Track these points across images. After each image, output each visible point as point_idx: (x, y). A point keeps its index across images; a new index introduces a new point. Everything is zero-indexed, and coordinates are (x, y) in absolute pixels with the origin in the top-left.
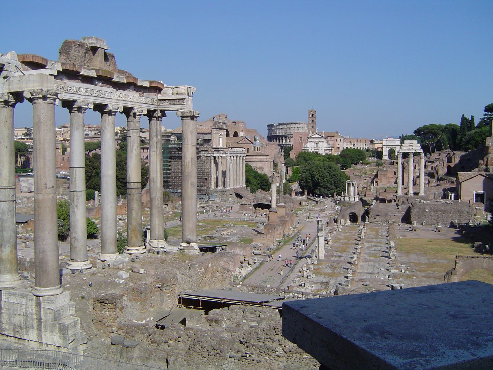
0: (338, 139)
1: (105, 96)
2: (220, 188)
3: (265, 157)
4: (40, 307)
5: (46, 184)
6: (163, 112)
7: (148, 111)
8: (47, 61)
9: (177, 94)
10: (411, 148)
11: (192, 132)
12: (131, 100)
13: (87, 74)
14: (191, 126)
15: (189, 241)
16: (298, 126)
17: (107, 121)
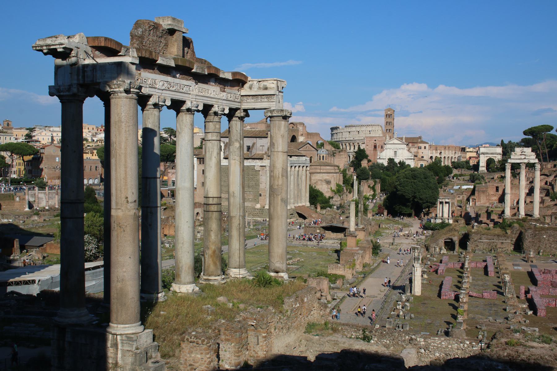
0: (423, 145)
1: (183, 91)
3: (332, 168)
4: (117, 349)
5: (127, 198)
6: (246, 110)
7: (230, 109)
8: (120, 45)
9: (266, 88)
10: (523, 157)
11: (283, 136)
12: (212, 96)
13: (165, 63)
14: (282, 128)
15: (278, 270)
16: (370, 128)
17: (184, 121)
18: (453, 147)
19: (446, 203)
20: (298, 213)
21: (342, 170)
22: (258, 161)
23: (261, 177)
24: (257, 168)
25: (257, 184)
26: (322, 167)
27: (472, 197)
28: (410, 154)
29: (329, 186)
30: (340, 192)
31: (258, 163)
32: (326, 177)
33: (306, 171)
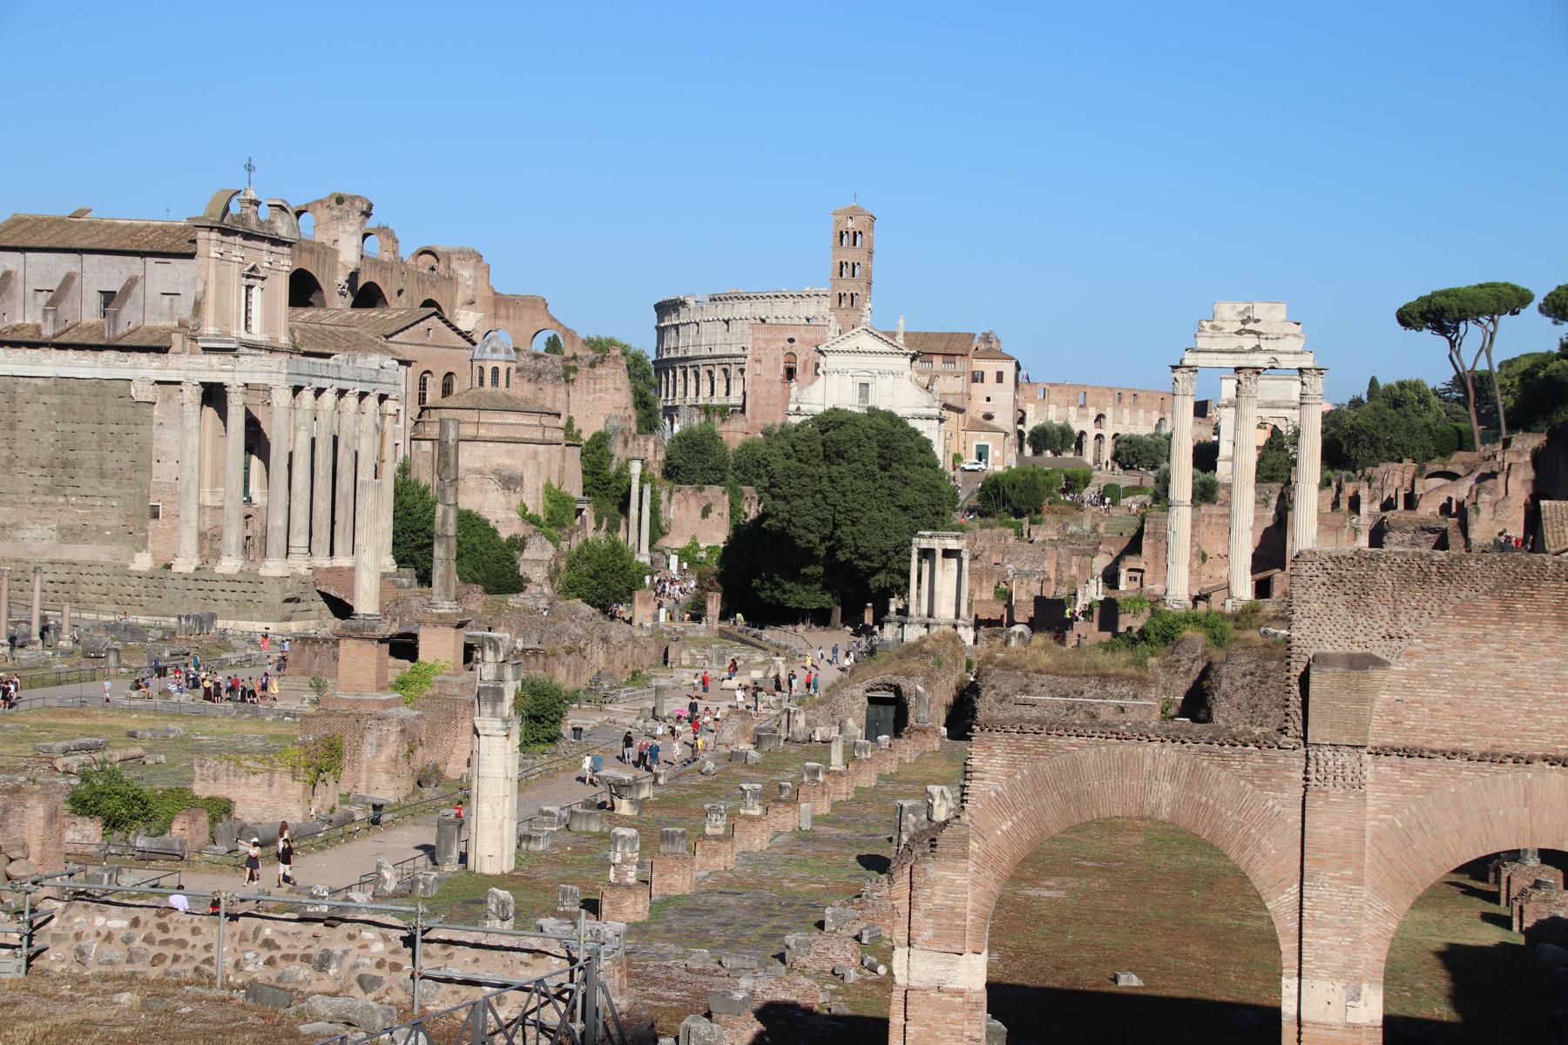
0: (989, 368)
2: (230, 564)
3: (534, 420)
10: (1249, 342)
18: (1151, 395)
19: (947, 553)
20: (327, 597)
21: (586, 436)
22: (143, 357)
23: (157, 432)
24: (141, 392)
25: (142, 465)
26: (486, 417)
27: (1131, 562)
28: (925, 398)
29: (515, 500)
30: (561, 526)
31: (143, 370)
32: (501, 457)
33: (383, 416)
